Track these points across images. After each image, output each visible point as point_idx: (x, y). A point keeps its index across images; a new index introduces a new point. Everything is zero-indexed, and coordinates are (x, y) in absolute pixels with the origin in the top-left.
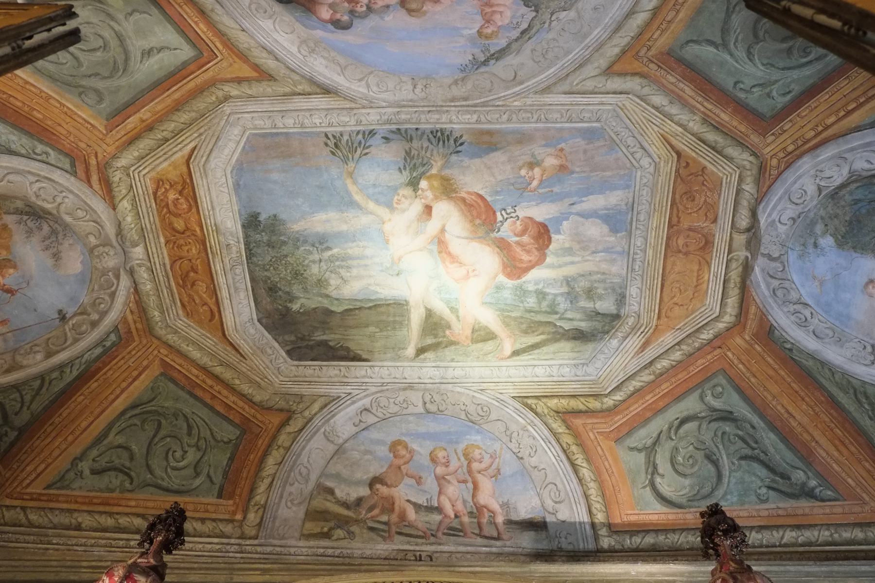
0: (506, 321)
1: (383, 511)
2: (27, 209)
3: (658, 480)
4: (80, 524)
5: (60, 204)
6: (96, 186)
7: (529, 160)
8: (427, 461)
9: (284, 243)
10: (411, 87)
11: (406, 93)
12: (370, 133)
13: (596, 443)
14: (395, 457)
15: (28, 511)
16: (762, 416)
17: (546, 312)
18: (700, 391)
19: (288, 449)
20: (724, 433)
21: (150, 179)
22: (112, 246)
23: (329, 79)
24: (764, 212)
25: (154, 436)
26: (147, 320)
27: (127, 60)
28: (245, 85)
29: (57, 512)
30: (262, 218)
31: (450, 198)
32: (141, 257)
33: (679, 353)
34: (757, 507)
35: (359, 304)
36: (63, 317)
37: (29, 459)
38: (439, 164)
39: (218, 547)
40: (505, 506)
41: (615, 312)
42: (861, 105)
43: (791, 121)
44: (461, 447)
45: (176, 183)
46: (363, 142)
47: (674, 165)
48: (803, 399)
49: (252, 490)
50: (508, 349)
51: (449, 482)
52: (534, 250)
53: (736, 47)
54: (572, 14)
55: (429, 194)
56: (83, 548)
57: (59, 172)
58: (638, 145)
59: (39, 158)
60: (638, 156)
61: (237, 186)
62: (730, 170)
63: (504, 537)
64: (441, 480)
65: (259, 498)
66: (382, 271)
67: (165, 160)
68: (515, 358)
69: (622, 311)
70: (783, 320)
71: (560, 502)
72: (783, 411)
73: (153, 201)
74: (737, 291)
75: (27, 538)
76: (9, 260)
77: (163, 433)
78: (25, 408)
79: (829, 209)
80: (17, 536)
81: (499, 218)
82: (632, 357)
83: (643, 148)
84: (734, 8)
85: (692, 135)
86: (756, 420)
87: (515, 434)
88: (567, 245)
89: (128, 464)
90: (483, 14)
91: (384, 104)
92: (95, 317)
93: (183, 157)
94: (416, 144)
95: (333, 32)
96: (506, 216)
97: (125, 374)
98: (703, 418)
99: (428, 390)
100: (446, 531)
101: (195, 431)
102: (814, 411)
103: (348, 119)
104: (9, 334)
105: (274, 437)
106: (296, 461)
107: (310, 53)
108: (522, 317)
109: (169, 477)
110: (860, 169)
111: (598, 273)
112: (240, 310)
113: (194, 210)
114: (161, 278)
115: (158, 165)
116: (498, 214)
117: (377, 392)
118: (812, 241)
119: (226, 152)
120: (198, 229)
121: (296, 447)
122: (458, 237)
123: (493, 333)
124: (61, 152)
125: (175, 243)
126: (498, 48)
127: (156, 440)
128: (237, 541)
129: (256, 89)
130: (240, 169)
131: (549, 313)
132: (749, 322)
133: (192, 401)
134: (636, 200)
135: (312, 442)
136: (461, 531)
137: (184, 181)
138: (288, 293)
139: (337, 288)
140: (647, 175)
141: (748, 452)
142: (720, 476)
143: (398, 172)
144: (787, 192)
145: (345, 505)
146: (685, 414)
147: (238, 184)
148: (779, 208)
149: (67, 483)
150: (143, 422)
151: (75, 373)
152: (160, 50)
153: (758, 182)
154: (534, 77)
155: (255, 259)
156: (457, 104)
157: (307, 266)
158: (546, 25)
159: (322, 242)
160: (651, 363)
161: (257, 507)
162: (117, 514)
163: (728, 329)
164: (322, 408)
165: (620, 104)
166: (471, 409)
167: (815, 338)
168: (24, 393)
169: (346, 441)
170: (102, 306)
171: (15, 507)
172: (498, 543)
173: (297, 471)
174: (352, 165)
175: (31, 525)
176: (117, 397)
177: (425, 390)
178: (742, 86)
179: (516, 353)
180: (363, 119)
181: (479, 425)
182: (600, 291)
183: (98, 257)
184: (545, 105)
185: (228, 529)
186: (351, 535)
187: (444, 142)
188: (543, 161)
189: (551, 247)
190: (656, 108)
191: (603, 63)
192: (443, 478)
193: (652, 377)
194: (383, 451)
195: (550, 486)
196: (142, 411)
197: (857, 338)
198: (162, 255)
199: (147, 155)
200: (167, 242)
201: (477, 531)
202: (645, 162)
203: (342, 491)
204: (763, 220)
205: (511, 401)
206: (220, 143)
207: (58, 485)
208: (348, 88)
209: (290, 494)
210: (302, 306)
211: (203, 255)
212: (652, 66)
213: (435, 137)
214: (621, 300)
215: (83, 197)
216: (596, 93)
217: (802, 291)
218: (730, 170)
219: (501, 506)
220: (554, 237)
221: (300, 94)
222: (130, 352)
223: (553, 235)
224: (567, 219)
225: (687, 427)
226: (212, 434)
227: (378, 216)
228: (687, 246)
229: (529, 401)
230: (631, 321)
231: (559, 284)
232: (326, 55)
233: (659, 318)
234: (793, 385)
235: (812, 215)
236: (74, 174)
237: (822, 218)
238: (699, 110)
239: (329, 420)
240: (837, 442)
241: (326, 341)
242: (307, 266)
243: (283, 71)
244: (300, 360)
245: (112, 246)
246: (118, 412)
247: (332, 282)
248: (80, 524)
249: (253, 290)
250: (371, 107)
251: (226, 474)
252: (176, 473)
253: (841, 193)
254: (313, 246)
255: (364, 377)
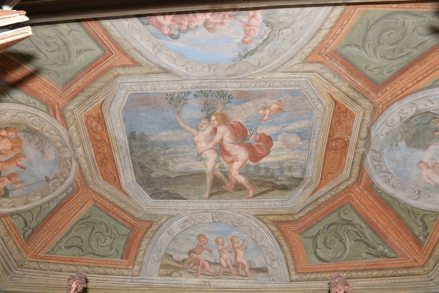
0: (251, 180)
1: (194, 265)
2: (28, 130)
3: (318, 250)
4: (62, 269)
5: (43, 127)
6: (59, 119)
7: (264, 106)
8: (214, 244)
9: (147, 146)
10: (207, 69)
11: (205, 73)
12: (188, 93)
13: (290, 235)
14: (200, 242)
15: (39, 263)
16: (366, 223)
17: (269, 177)
18: (338, 212)
19: (151, 238)
20: (348, 230)
21: (84, 116)
22: (68, 148)
23: (168, 65)
24: (374, 130)
25: (92, 232)
26: (86, 181)
27: (70, 56)
28: (127, 69)
29: (52, 264)
30: (137, 134)
31: (226, 124)
32: (81, 152)
33: (329, 195)
34: (362, 261)
35: (182, 174)
36: (48, 180)
37: (38, 241)
38: (221, 108)
39: (122, 280)
40: (249, 262)
41: (301, 177)
42: (424, 78)
43: (390, 86)
44: (230, 237)
45: (96, 117)
46: (184, 97)
47: (333, 108)
48: (384, 215)
49: (136, 256)
50: (251, 193)
51: (224, 252)
52: (265, 149)
53: (369, 48)
54: (290, 30)
55: (216, 122)
56: (64, 279)
57: (41, 112)
58: (316, 98)
59: (32, 105)
60: (316, 103)
61: (125, 119)
62: (359, 110)
63: (249, 276)
64: (221, 252)
65: (139, 259)
66: (193, 159)
67: (91, 106)
68: (254, 198)
69: (304, 176)
70: (378, 180)
71: (274, 260)
72: (375, 220)
73: (85, 126)
74: (358, 167)
75: (40, 274)
76: (22, 154)
77: (95, 231)
78: (34, 220)
79: (405, 128)
80: (36, 274)
81: (249, 134)
82: (308, 197)
83: (319, 99)
84: (370, 27)
85: (343, 93)
86: (363, 224)
87: (254, 232)
88: (280, 146)
89: (80, 244)
90: (245, 31)
91: (195, 78)
92: (62, 180)
93: (99, 104)
94: (210, 98)
95: (170, 41)
96: (252, 133)
97: (77, 205)
98: (339, 223)
99: (214, 212)
100: (223, 273)
101: (109, 230)
102: (389, 220)
103: (177, 86)
104: (24, 187)
105: (145, 233)
106: (155, 243)
107: (158, 52)
108: (258, 180)
109: (99, 250)
110: (421, 109)
111: (294, 159)
112: (128, 177)
113: (105, 130)
114: (91, 162)
115: (87, 109)
116: (248, 132)
117: (191, 213)
118: (396, 143)
119: (119, 102)
120: (107, 139)
121: (155, 237)
122: (229, 143)
123: (245, 187)
124: (41, 102)
125: (96, 146)
126: (251, 49)
127: (93, 234)
128: (130, 277)
129: (133, 70)
130: (125, 110)
131: (271, 178)
132: (363, 181)
133: (108, 217)
134: (314, 124)
135: (162, 235)
136: (229, 273)
137: (100, 117)
138: (150, 169)
139: (172, 167)
140: (320, 113)
141: (358, 238)
142: (345, 249)
143: (201, 112)
144: (386, 121)
145: (178, 262)
146: (331, 222)
147: (125, 118)
148: (381, 128)
149: (55, 252)
150: (86, 226)
151: (55, 205)
152: (86, 50)
153: (372, 115)
154: (268, 64)
155: (134, 153)
156: (230, 78)
157: (158, 156)
158: (276, 37)
159: (165, 145)
160: (316, 200)
161: (138, 263)
162: (77, 265)
163: (352, 184)
164: (166, 220)
165: (309, 77)
166: (234, 220)
167: (392, 187)
168: (33, 213)
169: (178, 235)
170: (65, 175)
171: (34, 261)
172: (246, 278)
173: (156, 248)
174: (179, 108)
175: (41, 269)
176: (74, 215)
177: (213, 212)
178: (369, 68)
179: (254, 196)
180: (184, 86)
181: (238, 227)
182: (295, 167)
183: (62, 152)
184: (273, 78)
185: (126, 272)
186: (181, 275)
187: (223, 97)
188: (270, 106)
189: (273, 147)
190: (327, 80)
191: (303, 57)
192: (222, 250)
193: (317, 206)
194: (194, 239)
195: (269, 254)
196: (85, 221)
197: (412, 187)
198: (90, 152)
199: (82, 104)
200: (93, 146)
201: (237, 273)
202: (320, 106)
203: (176, 256)
204: (373, 134)
205: (252, 217)
206: (116, 98)
207: (51, 252)
208: (177, 70)
209: (153, 257)
210: (156, 175)
211: (110, 151)
212: (327, 58)
213: (219, 95)
214: (304, 171)
215: (53, 124)
216: (298, 72)
217: (389, 167)
218: (359, 110)
219: (247, 262)
220: (274, 143)
221: (153, 73)
222: (79, 196)
223: (273, 142)
224: (280, 134)
225: (331, 227)
226: (117, 232)
227: (191, 133)
228: (336, 146)
229: (261, 217)
230: (308, 181)
231: (276, 164)
232: (166, 53)
233: (321, 179)
234: (380, 208)
235: (396, 131)
236: (48, 113)
237: (401, 133)
238: (347, 81)
239: (170, 225)
240: (398, 233)
241: (168, 191)
242: (158, 156)
243: (145, 61)
244: (156, 199)
245: (68, 148)
246: (75, 222)
247: (170, 164)
248: (62, 269)
249: (133, 168)
250: (189, 80)
251: (124, 249)
252: (102, 248)
253: (411, 121)
254: (161, 147)
255: (185, 207)
